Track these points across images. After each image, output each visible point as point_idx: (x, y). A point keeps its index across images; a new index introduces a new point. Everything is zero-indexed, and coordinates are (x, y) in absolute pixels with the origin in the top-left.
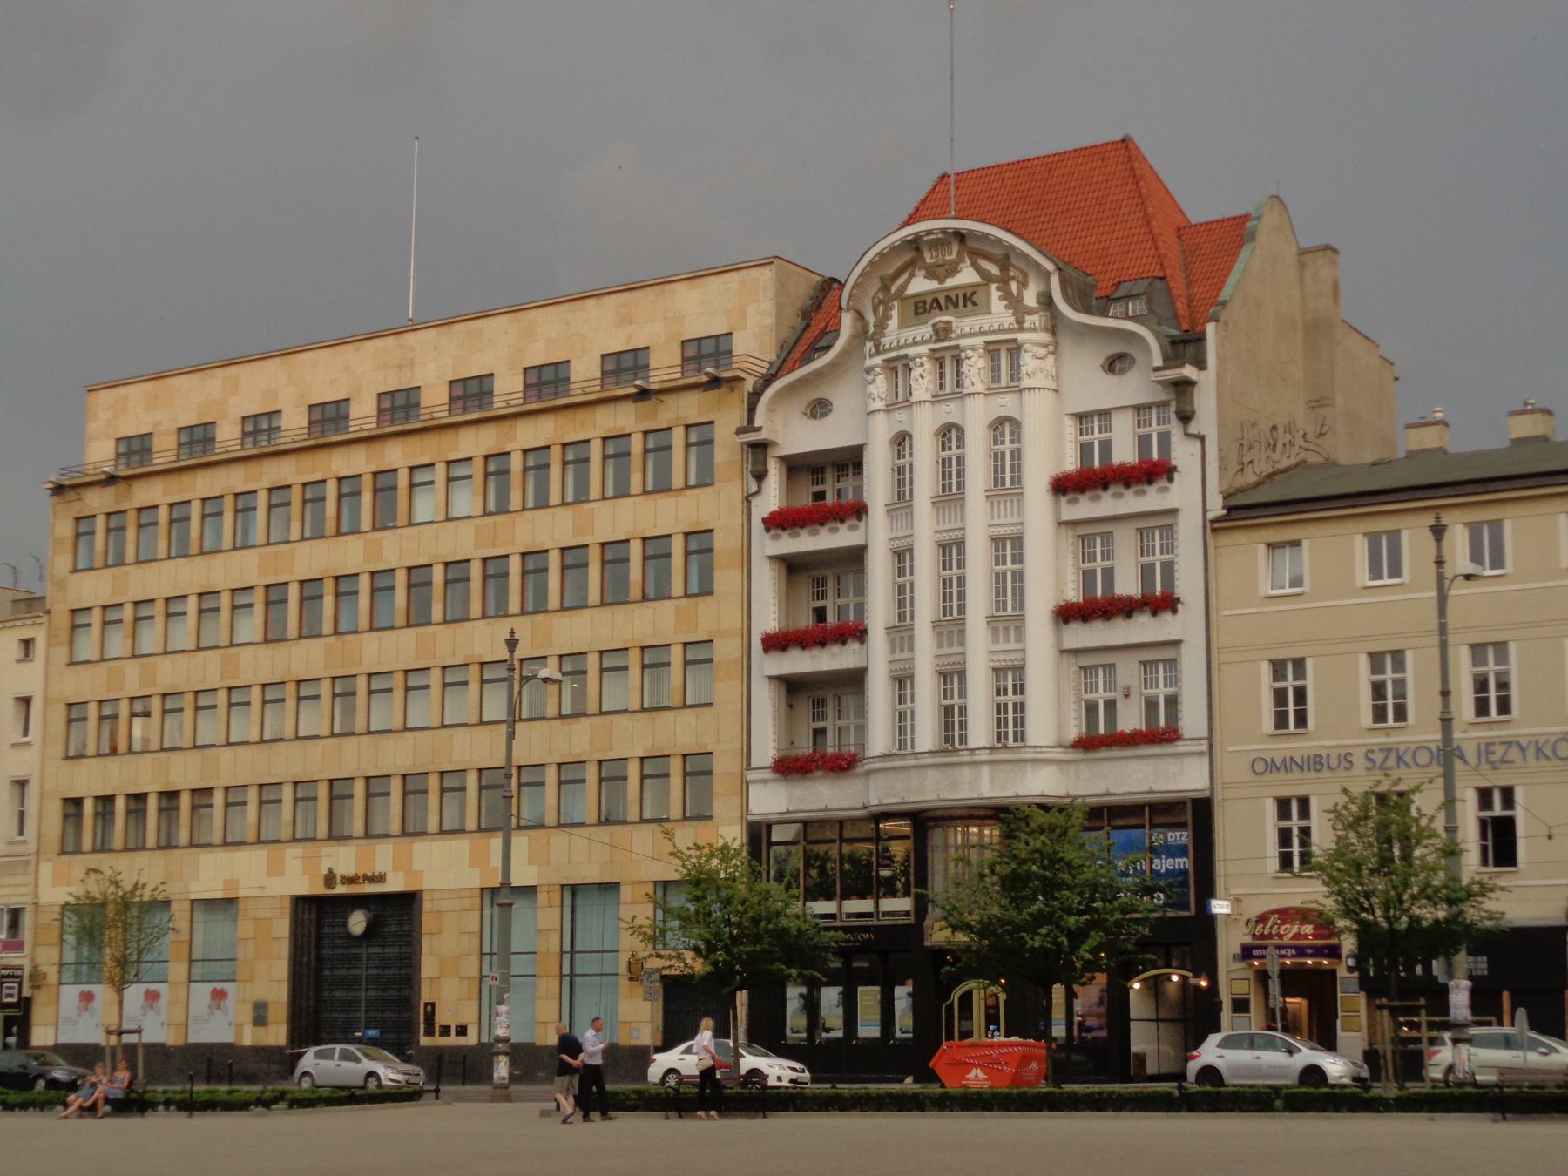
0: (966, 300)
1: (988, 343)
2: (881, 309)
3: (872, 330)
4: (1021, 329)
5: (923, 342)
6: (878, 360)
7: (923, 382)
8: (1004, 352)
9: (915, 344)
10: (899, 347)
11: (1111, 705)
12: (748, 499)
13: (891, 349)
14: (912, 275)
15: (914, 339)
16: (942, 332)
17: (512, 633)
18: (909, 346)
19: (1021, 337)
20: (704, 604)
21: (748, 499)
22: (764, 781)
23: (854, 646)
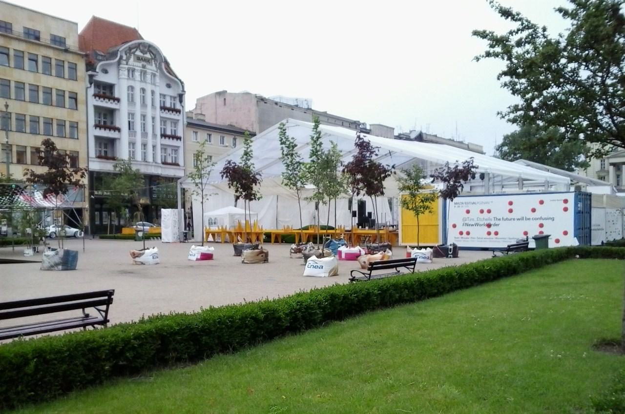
0: (148, 61)
1: (152, 73)
2: (128, 54)
3: (125, 57)
4: (157, 72)
5: (140, 67)
6: (127, 66)
7: (137, 74)
8: (154, 75)
9: (138, 66)
10: (133, 66)
11: (165, 157)
12: (87, 88)
13: (131, 65)
14: (137, 50)
15: (138, 65)
16: (144, 67)
17: (6, 103)
18: (136, 66)
19: (156, 73)
20: (75, 112)
21: (87, 88)
22: (94, 161)
23: (117, 132)
